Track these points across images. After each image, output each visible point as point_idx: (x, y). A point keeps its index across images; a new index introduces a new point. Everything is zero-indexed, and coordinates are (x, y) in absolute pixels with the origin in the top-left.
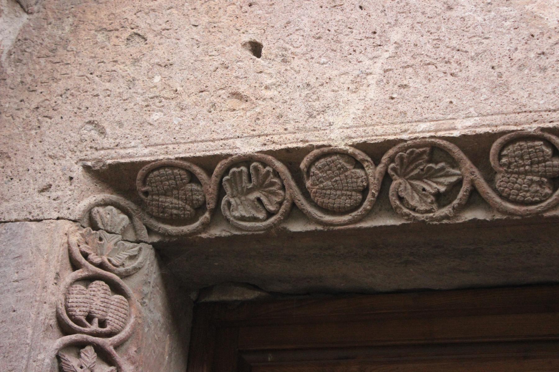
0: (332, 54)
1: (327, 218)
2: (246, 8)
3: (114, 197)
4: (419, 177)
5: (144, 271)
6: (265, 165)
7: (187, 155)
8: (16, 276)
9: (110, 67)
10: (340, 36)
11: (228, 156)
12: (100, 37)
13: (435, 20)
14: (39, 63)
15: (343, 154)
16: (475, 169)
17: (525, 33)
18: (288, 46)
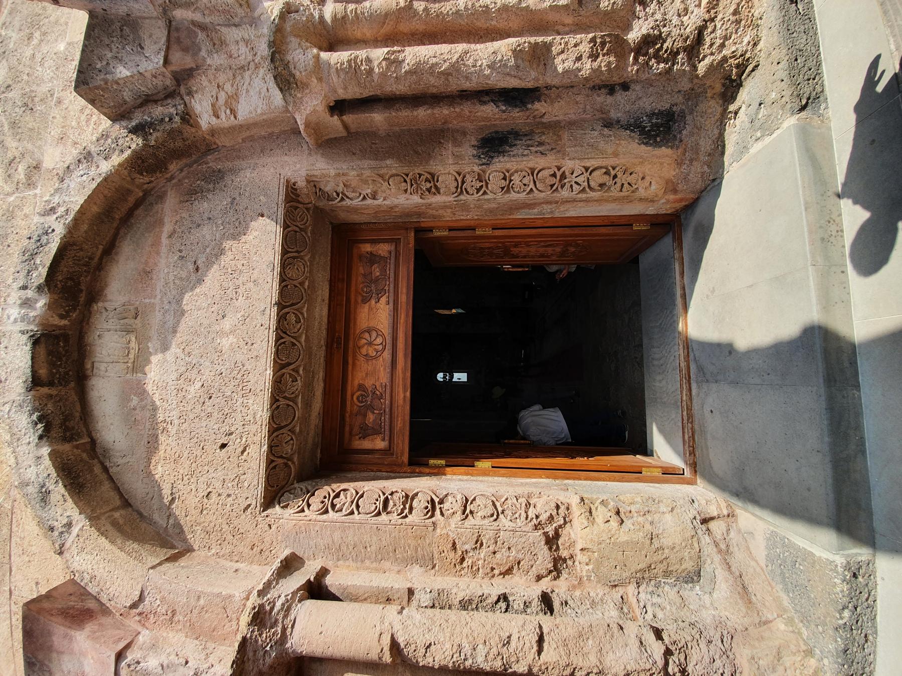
1: (296, 419)
2: (204, 451)
3: (277, 499)
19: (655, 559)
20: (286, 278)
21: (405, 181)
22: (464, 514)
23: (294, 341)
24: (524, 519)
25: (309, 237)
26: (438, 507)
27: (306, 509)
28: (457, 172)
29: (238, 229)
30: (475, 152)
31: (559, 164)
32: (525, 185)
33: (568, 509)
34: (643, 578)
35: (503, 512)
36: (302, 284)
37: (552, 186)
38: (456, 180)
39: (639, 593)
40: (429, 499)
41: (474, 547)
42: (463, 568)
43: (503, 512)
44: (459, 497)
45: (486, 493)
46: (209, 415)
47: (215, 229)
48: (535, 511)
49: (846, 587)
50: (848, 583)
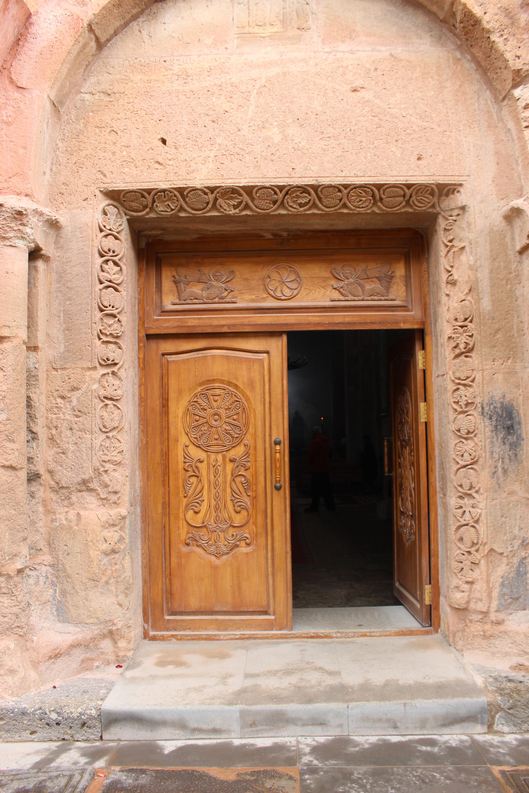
0: (194, 147)
2: (158, 122)
4: (227, 199)
5: (125, 230)
6: (171, 192)
7: (141, 188)
8: (81, 236)
9: (104, 145)
10: (197, 139)
11: (156, 189)
12: (97, 130)
13: (234, 135)
14: (72, 141)
15: (200, 190)
16: (247, 197)
17: (267, 144)
18: (177, 142)
19: (76, 582)
20: (348, 189)
21: (466, 319)
22: (104, 397)
23: (278, 203)
24: (103, 459)
25: (399, 209)
26: (109, 370)
27: (103, 234)
28: (474, 378)
29: (403, 133)
30: (497, 399)
31: (481, 491)
32: (462, 456)
33: (115, 503)
34: (58, 571)
35: (108, 437)
36: (345, 206)
37: (461, 486)
38: (468, 378)
39: (46, 565)
40: (116, 361)
41: (75, 409)
42: (55, 399)
43: (108, 437)
44: (119, 392)
45: (124, 419)
46: (195, 123)
47: (403, 106)
48: (110, 470)
49: (75, 715)
50: (78, 717)
